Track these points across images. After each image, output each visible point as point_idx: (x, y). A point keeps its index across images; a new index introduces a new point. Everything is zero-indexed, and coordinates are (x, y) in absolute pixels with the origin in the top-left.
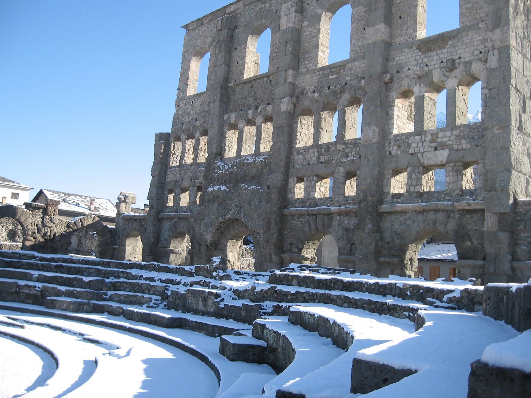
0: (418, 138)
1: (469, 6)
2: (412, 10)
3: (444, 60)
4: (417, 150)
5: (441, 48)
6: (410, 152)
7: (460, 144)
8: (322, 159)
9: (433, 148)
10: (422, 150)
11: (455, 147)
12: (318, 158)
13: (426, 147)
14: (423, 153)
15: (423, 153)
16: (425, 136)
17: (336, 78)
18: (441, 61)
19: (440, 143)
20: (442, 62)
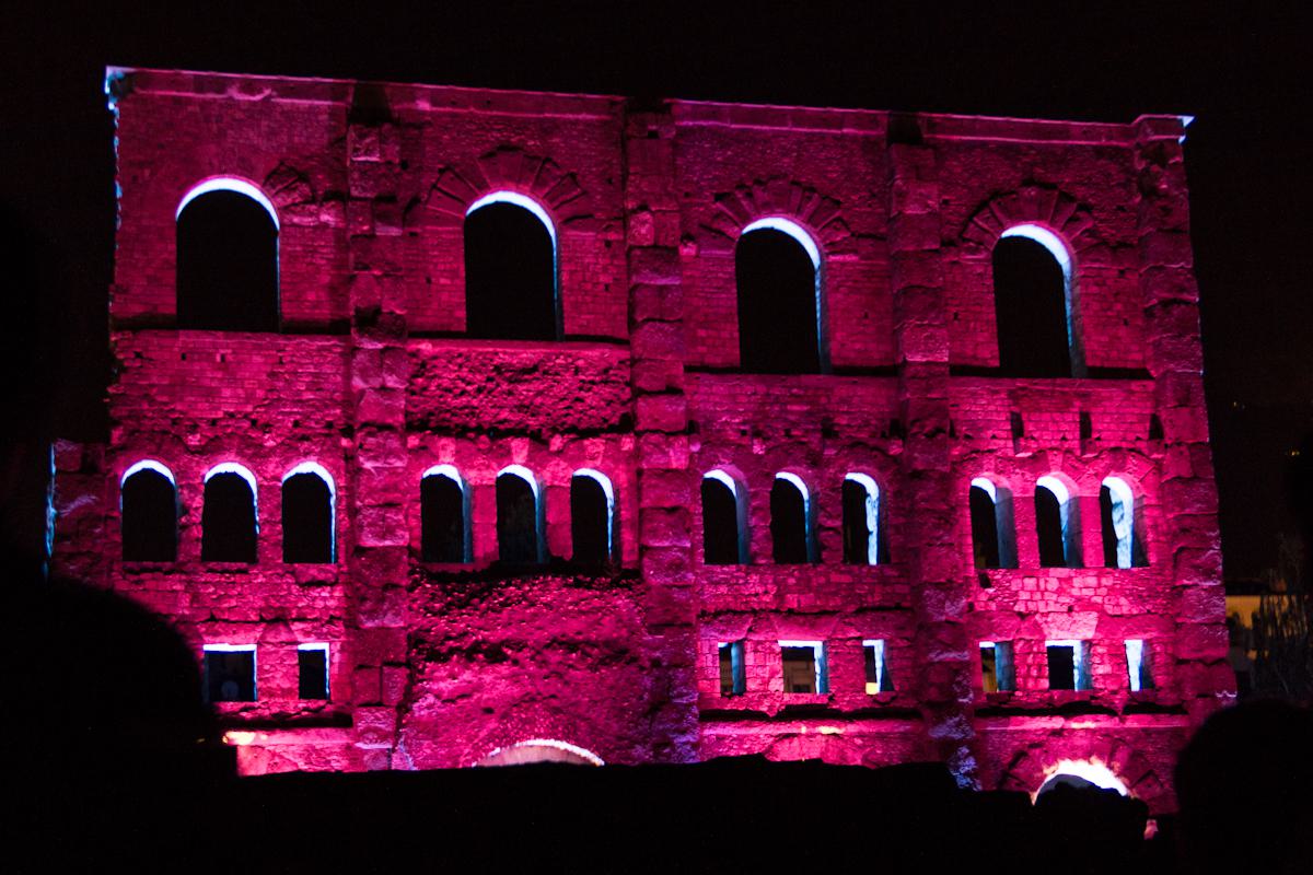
0: (1030, 582)
1: (1104, 339)
2: (984, 308)
3: (1069, 436)
4: (1032, 606)
5: (1061, 411)
6: (1016, 608)
7: (1118, 605)
8: (792, 601)
9: (1065, 608)
10: (1042, 609)
11: (1110, 610)
12: (780, 596)
13: (1051, 603)
14: (1046, 615)
15: (1046, 615)
16: (1046, 581)
17: (807, 412)
18: (1062, 435)
19: (1079, 599)
20: (1064, 439)
